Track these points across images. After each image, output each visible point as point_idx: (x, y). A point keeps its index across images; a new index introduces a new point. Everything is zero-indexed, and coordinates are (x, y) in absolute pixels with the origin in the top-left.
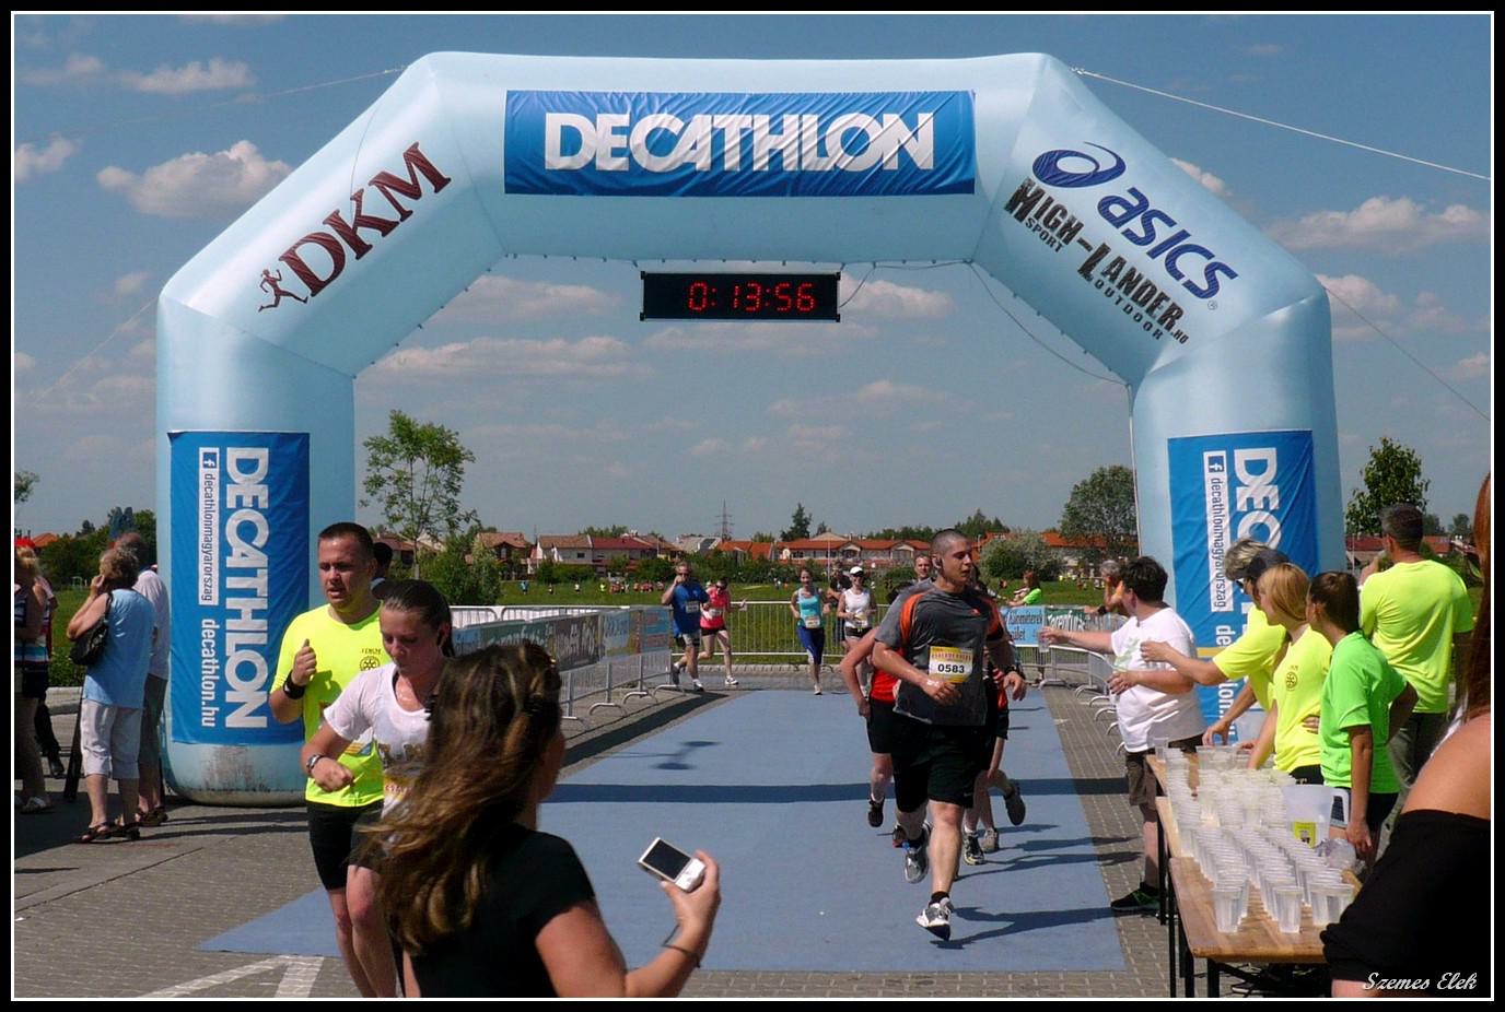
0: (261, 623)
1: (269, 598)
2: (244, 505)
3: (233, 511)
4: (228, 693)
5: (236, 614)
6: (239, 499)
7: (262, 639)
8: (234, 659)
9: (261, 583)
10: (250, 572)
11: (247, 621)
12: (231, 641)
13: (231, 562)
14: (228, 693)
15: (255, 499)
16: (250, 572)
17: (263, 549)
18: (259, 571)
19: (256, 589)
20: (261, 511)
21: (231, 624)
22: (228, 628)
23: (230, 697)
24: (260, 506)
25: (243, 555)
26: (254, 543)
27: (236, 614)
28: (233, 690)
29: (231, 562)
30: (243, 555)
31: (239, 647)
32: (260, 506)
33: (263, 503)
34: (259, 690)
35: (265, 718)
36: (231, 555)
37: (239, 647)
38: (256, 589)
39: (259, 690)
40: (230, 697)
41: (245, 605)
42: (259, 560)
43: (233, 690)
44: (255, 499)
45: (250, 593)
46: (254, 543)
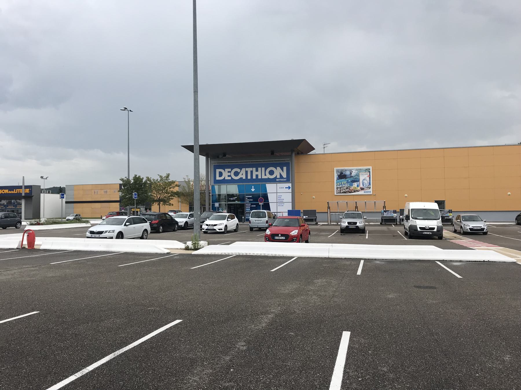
0: (259, 169)
3: (232, 178)
4: (277, 178)
5: (257, 176)
6: (229, 176)
7: (263, 169)
8: (268, 176)
9: (249, 170)
10: (247, 172)
11: (259, 173)
12: (264, 177)
13: (244, 178)
15: (229, 172)
16: (247, 172)
20: (231, 170)
21: (260, 177)
25: (242, 175)
27: (257, 176)
28: (277, 176)
29: (244, 178)
30: (242, 175)
31: (265, 175)
33: (230, 170)
36: (242, 178)
37: (265, 175)
40: (278, 177)
42: (243, 170)
43: (277, 176)
44: (229, 172)
45: (252, 172)
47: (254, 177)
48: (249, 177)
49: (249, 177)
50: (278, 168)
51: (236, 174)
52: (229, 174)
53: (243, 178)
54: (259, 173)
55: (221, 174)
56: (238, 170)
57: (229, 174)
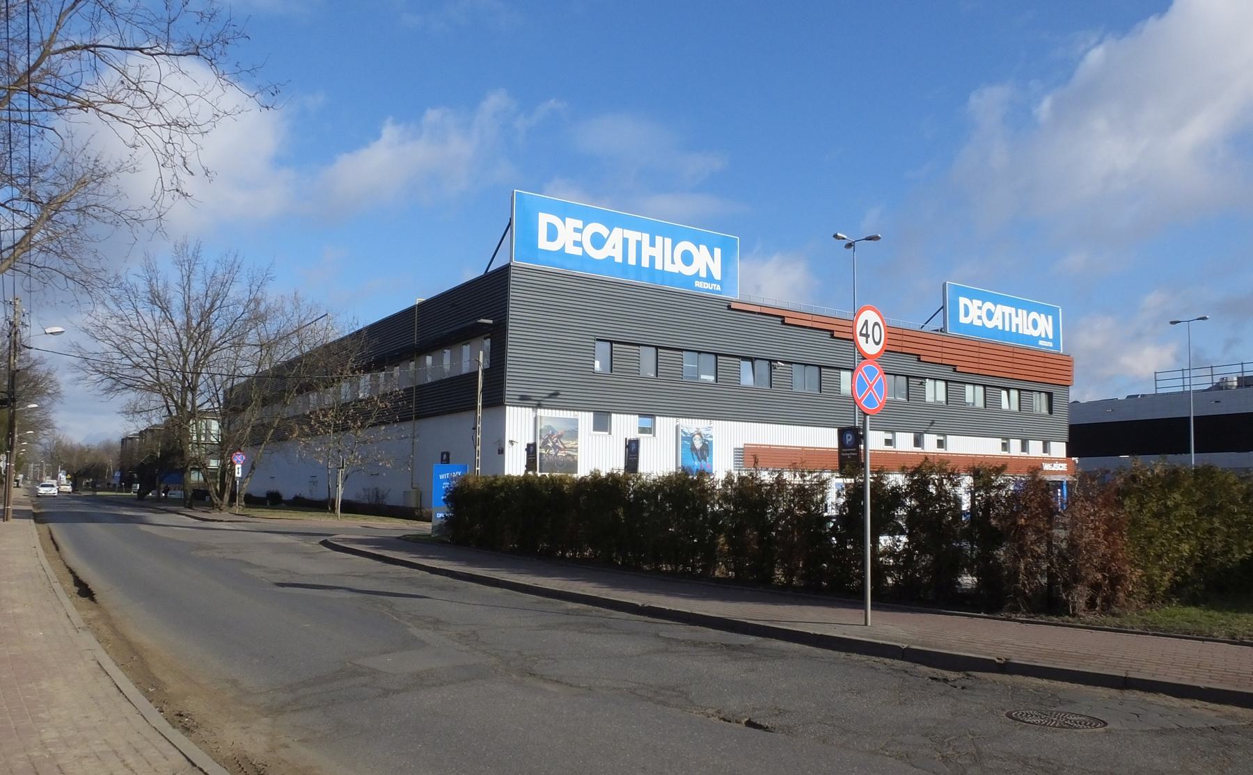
0: (659, 239)
1: (642, 231)
2: (580, 240)
3: (583, 250)
4: (701, 275)
5: (652, 259)
6: (578, 244)
7: (668, 241)
8: (679, 267)
9: (633, 236)
10: (625, 241)
11: (656, 252)
12: (669, 268)
13: (619, 259)
14: (701, 275)
15: (576, 230)
16: (625, 241)
17: (611, 231)
18: (625, 236)
19: (637, 241)
20: (584, 227)
21: (658, 266)
22: (661, 269)
23: (703, 274)
24: (581, 227)
25: (614, 247)
26: (606, 238)
27: (652, 259)
28: (699, 270)
29: (619, 259)
30: (614, 247)
31: (673, 262)
32: (581, 227)
34: (699, 249)
35: (715, 249)
36: (614, 257)
37: (673, 262)
38: (637, 241)
39: (699, 249)
40: (703, 274)
41: (647, 251)
43: (699, 270)
44: (576, 230)
45: (639, 244)
46: (606, 238)
47: (645, 263)
48: (632, 261)
49: (632, 261)
50: (703, 248)
51: (598, 242)
52: (577, 237)
53: (616, 260)
54: (656, 252)
55: (552, 234)
56: (604, 231)
57: (577, 237)
